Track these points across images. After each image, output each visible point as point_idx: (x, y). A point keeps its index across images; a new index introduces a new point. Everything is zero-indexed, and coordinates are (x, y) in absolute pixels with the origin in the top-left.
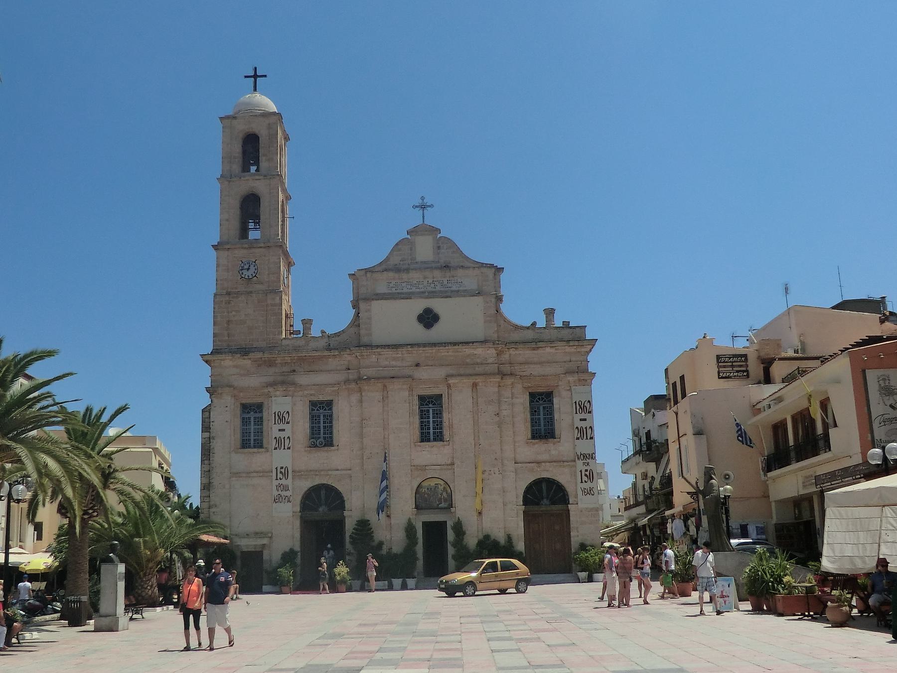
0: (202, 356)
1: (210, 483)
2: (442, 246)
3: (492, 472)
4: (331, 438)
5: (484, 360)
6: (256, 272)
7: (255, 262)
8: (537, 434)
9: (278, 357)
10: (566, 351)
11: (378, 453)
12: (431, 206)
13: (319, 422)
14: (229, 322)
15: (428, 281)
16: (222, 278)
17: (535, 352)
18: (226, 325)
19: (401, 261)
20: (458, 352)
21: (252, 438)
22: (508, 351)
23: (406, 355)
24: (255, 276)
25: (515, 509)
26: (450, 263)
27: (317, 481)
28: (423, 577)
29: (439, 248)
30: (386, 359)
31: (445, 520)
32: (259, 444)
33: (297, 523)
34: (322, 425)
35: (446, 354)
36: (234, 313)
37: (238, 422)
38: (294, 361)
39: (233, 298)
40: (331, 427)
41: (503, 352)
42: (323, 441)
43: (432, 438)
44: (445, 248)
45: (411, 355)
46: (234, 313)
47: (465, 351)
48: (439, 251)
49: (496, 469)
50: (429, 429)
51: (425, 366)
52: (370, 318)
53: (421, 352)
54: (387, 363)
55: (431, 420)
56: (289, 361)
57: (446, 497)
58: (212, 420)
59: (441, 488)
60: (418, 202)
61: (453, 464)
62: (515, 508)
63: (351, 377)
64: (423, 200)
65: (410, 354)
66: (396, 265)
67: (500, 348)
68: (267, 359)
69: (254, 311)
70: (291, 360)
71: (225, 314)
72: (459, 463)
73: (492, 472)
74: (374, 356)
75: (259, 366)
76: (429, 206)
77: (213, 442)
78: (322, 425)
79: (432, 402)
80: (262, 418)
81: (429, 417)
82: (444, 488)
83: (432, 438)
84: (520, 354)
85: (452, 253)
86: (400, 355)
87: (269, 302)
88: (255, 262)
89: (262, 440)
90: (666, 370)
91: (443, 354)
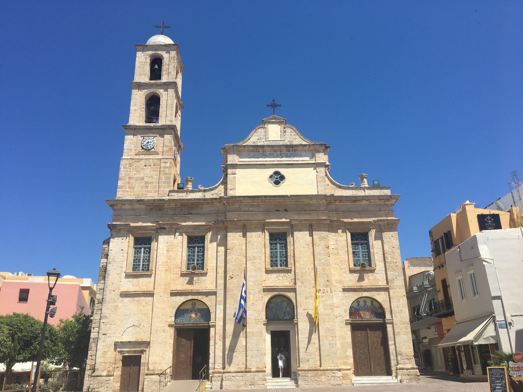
0: (107, 201)
1: (103, 298)
2: (287, 130)
3: (326, 291)
4: (203, 264)
5: (317, 208)
6: (154, 145)
7: (153, 138)
8: (357, 263)
9: (166, 203)
10: (377, 203)
11: (238, 275)
12: (280, 106)
13: (194, 252)
14: (130, 178)
15: (277, 154)
16: (128, 148)
17: (354, 203)
18: (128, 181)
19: (258, 139)
20: (298, 202)
21: (141, 264)
22: (335, 202)
23: (260, 203)
24: (153, 148)
25: (345, 321)
26: (293, 142)
27: (190, 297)
28: (271, 378)
29: (285, 132)
30: (246, 206)
31: (289, 330)
32: (147, 268)
33: (171, 332)
34: (196, 254)
35: (290, 203)
36: (135, 172)
37: (132, 251)
38: (178, 206)
39: (135, 162)
40: (203, 256)
41: (331, 203)
42: (196, 266)
43: (279, 264)
44: (289, 132)
45: (264, 203)
46: (135, 172)
47: (304, 201)
48: (285, 134)
49: (329, 289)
50: (276, 257)
51: (274, 212)
52: (235, 177)
53: (272, 201)
54: (246, 209)
55: (279, 250)
56: (174, 207)
57: (289, 311)
58: (110, 248)
59: (285, 304)
60: (270, 102)
61: (295, 284)
62: (344, 320)
63: (220, 219)
64: (274, 101)
65: (263, 202)
66: (255, 142)
67: (329, 200)
68: (157, 204)
69: (150, 171)
70: (175, 205)
71: (129, 172)
72: (300, 284)
73: (326, 291)
74: (237, 204)
75: (151, 209)
76: (278, 105)
77: (109, 266)
78: (196, 254)
79: (279, 238)
80: (150, 248)
81: (276, 249)
82: (288, 304)
83: (279, 264)
84: (343, 205)
85: (294, 136)
86: (256, 203)
87: (163, 165)
88: (153, 138)
89: (148, 265)
90: (430, 232)
91: (287, 203)
